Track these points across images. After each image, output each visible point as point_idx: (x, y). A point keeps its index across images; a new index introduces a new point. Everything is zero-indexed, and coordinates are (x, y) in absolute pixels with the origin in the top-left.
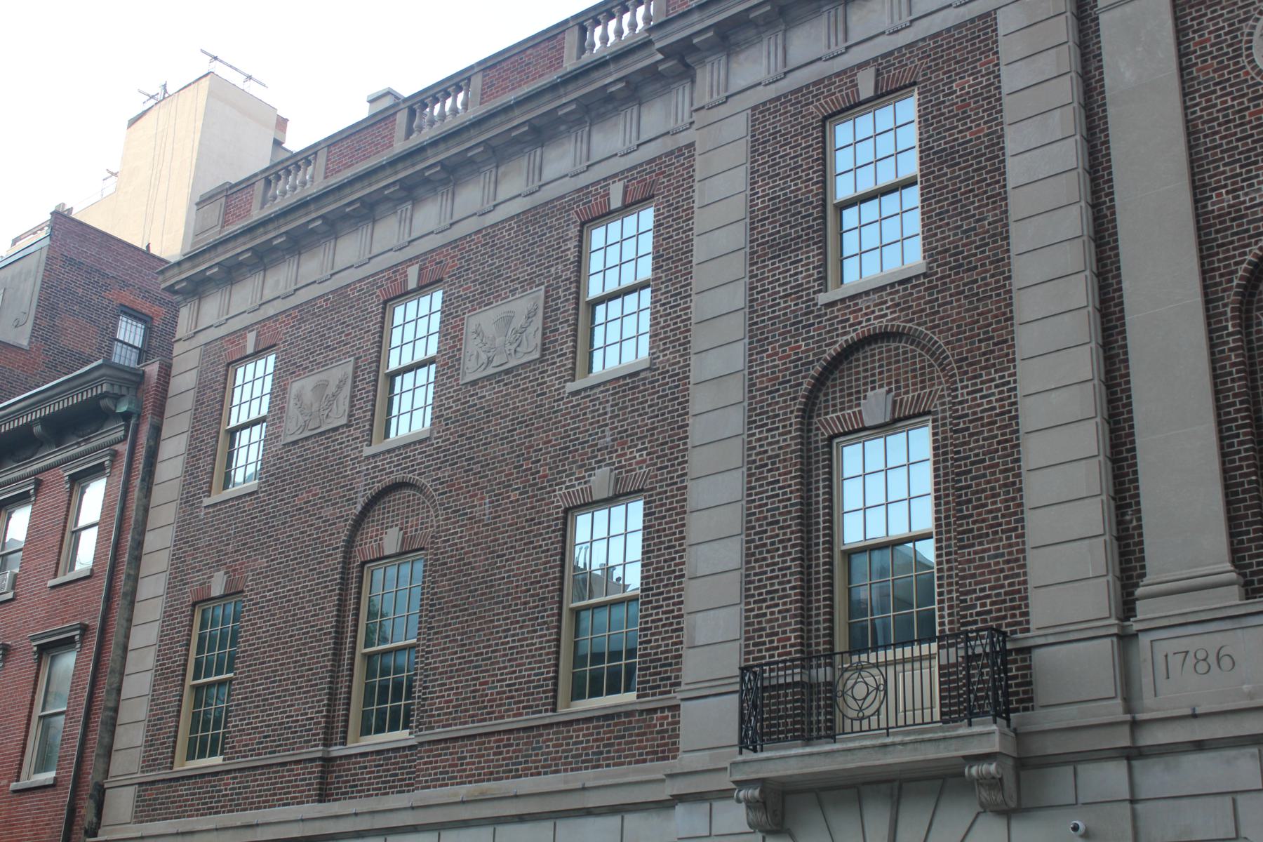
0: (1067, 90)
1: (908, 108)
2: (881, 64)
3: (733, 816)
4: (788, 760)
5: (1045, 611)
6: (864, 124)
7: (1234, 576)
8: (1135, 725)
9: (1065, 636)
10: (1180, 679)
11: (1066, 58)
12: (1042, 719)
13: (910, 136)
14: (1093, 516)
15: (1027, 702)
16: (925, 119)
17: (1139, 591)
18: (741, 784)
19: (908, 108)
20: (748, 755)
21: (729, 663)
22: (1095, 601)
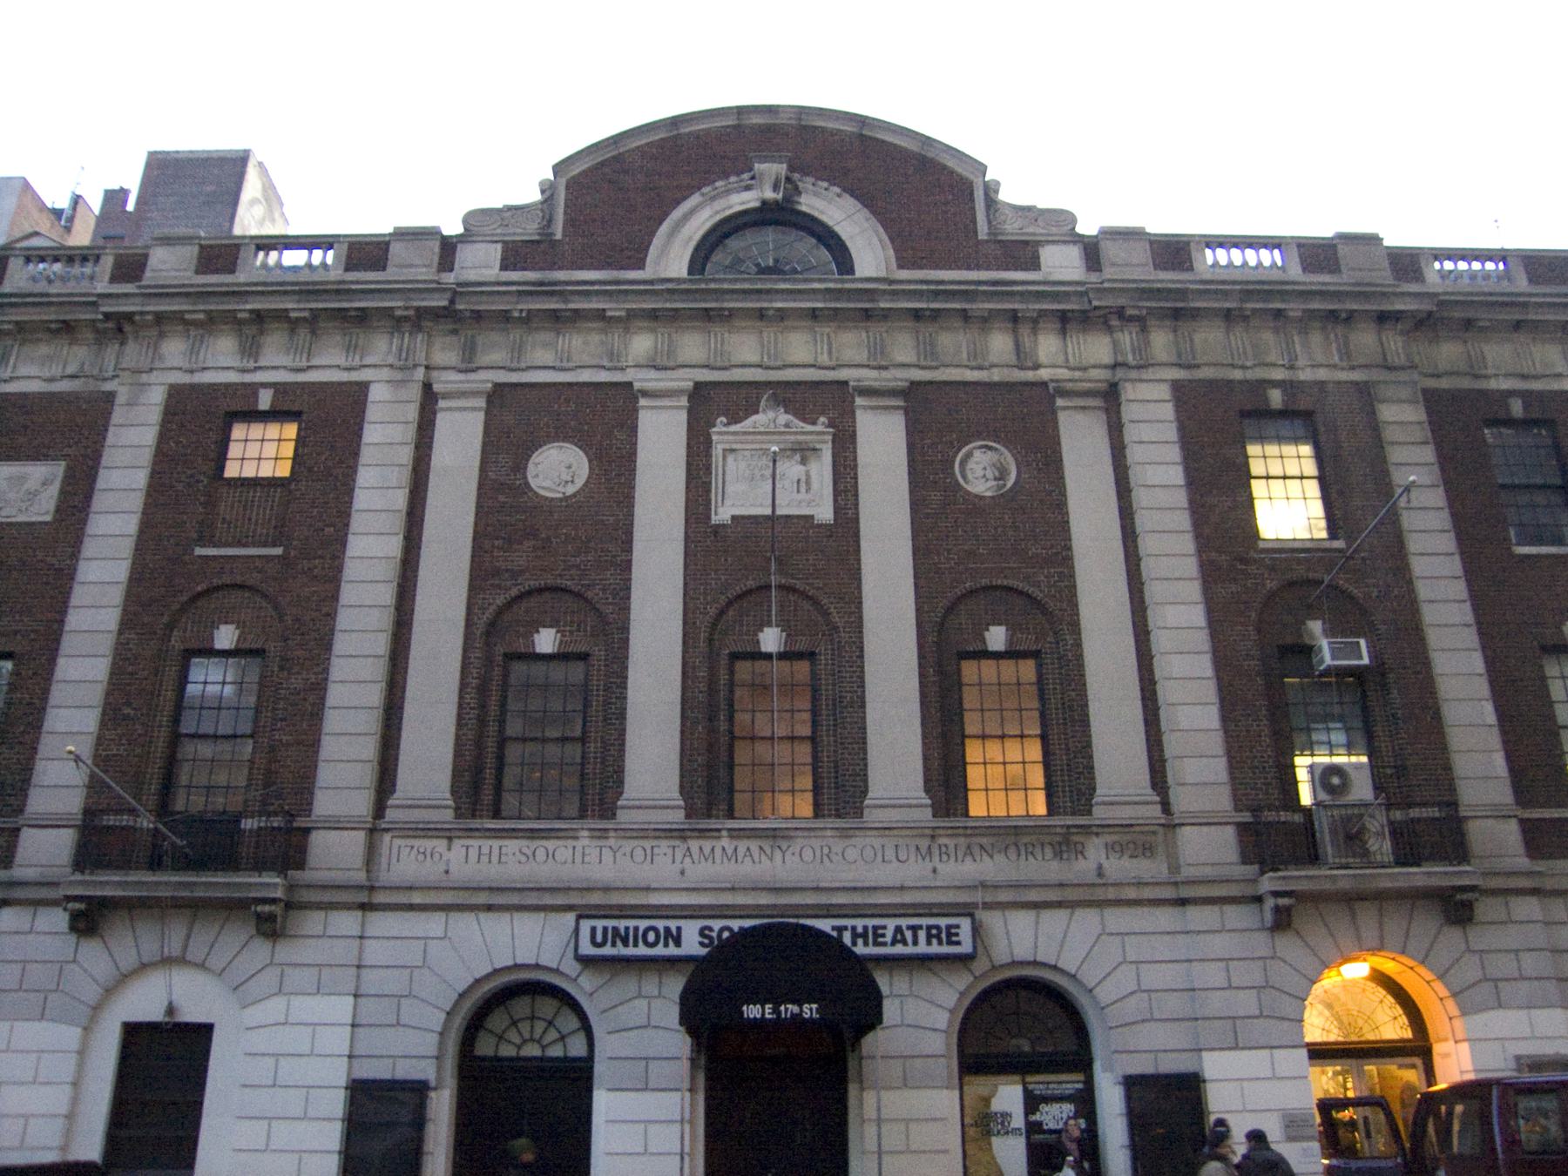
0: (406, 455)
1: (291, 430)
2: (280, 389)
3: (58, 919)
4: (109, 884)
5: (325, 804)
6: (256, 430)
7: (450, 803)
8: (372, 888)
9: (336, 825)
10: (406, 861)
11: (410, 433)
12: (306, 876)
13: (288, 450)
14: (369, 749)
15: (301, 865)
16: (300, 441)
17: (390, 802)
18: (69, 899)
19: (291, 430)
20: (78, 877)
21: (72, 803)
22: (361, 804)
